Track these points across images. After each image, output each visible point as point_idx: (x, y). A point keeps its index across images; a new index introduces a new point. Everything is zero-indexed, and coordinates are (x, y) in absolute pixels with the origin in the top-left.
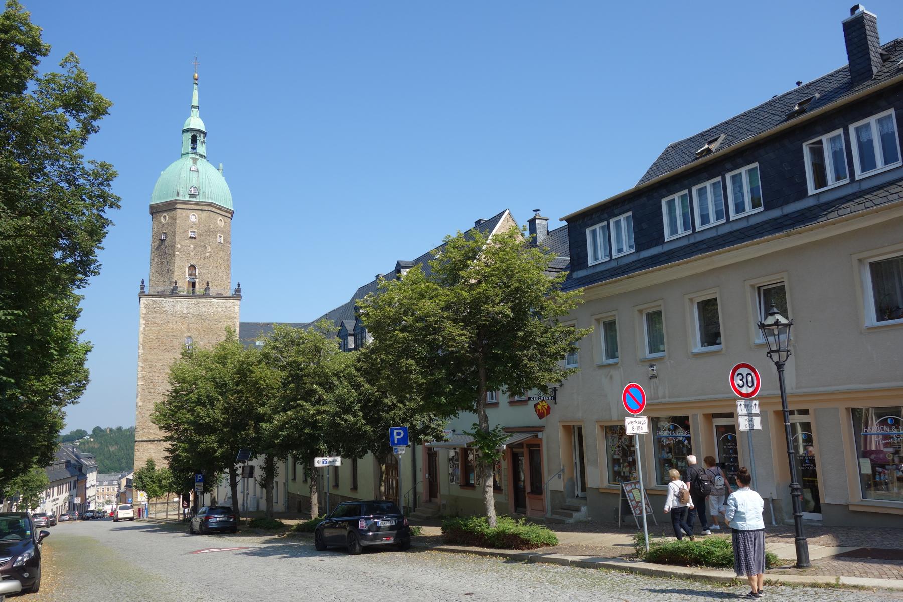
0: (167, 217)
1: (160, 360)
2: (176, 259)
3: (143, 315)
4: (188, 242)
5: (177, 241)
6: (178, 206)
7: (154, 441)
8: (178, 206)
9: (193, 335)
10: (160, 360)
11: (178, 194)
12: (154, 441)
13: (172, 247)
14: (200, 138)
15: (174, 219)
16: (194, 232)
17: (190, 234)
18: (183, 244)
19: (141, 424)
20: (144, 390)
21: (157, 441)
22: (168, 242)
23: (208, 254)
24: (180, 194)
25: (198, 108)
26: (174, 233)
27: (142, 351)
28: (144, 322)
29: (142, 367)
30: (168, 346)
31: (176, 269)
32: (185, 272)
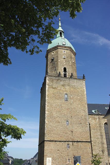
0: (54, 52)
1: (55, 103)
2: (59, 65)
3: (48, 84)
4: (63, 60)
5: (59, 59)
6: (59, 48)
7: (53, 141)
8: (59, 48)
9: (68, 93)
10: (55, 103)
11: (58, 44)
12: (53, 141)
13: (57, 61)
14: (63, 34)
15: (57, 52)
16: (65, 56)
17: (63, 57)
18: (61, 60)
19: (47, 132)
20: (48, 116)
21: (55, 141)
22: (55, 60)
23: (70, 64)
24: (59, 44)
25: (61, 26)
26: (57, 57)
27: (47, 98)
28: (48, 86)
29: (47, 105)
30: (58, 97)
31: (59, 68)
32: (62, 70)
